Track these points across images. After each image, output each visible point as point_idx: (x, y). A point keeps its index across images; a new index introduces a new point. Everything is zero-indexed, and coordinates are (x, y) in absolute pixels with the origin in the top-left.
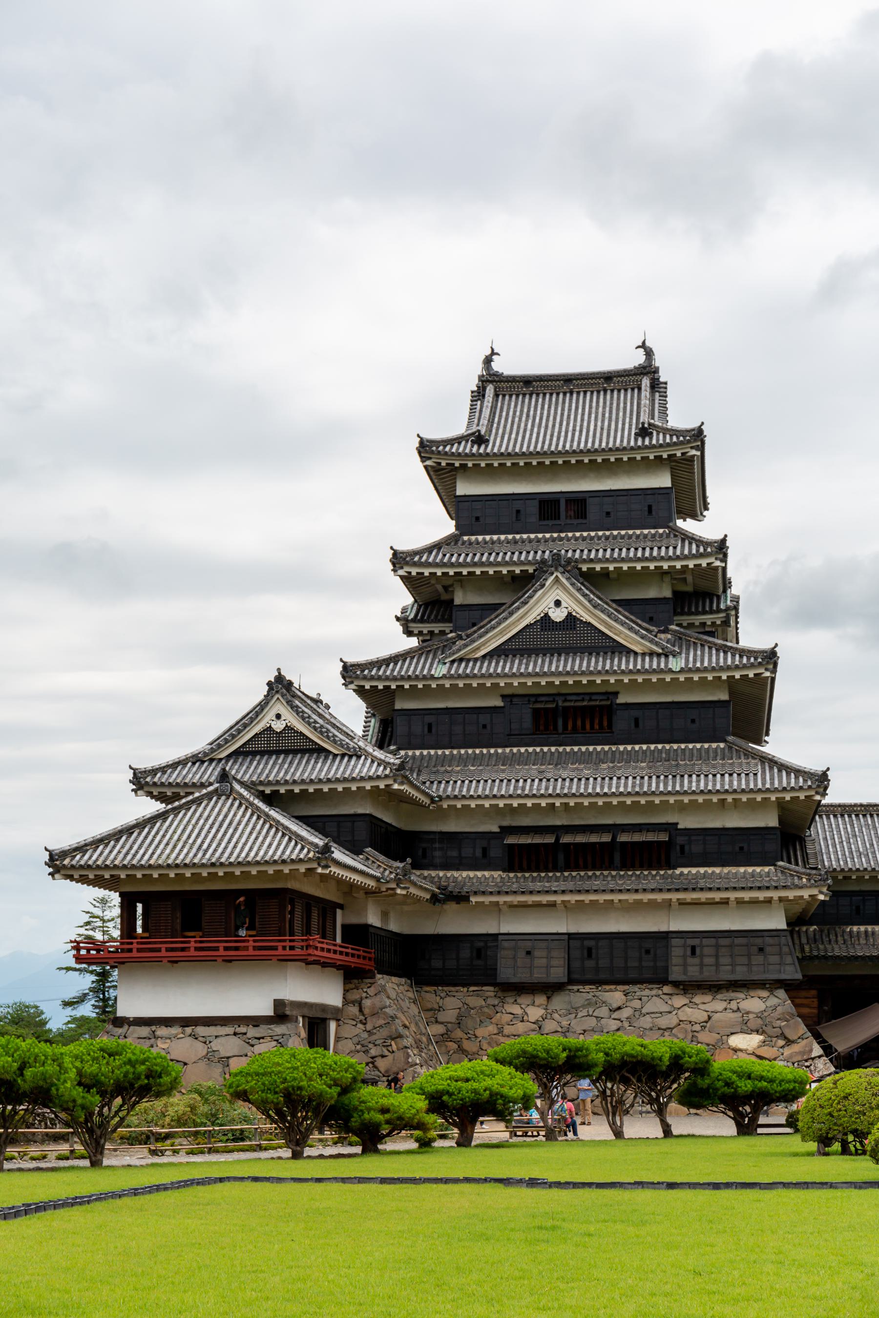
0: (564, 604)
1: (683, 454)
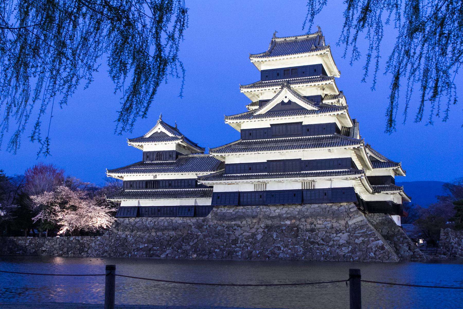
0: (287, 97)
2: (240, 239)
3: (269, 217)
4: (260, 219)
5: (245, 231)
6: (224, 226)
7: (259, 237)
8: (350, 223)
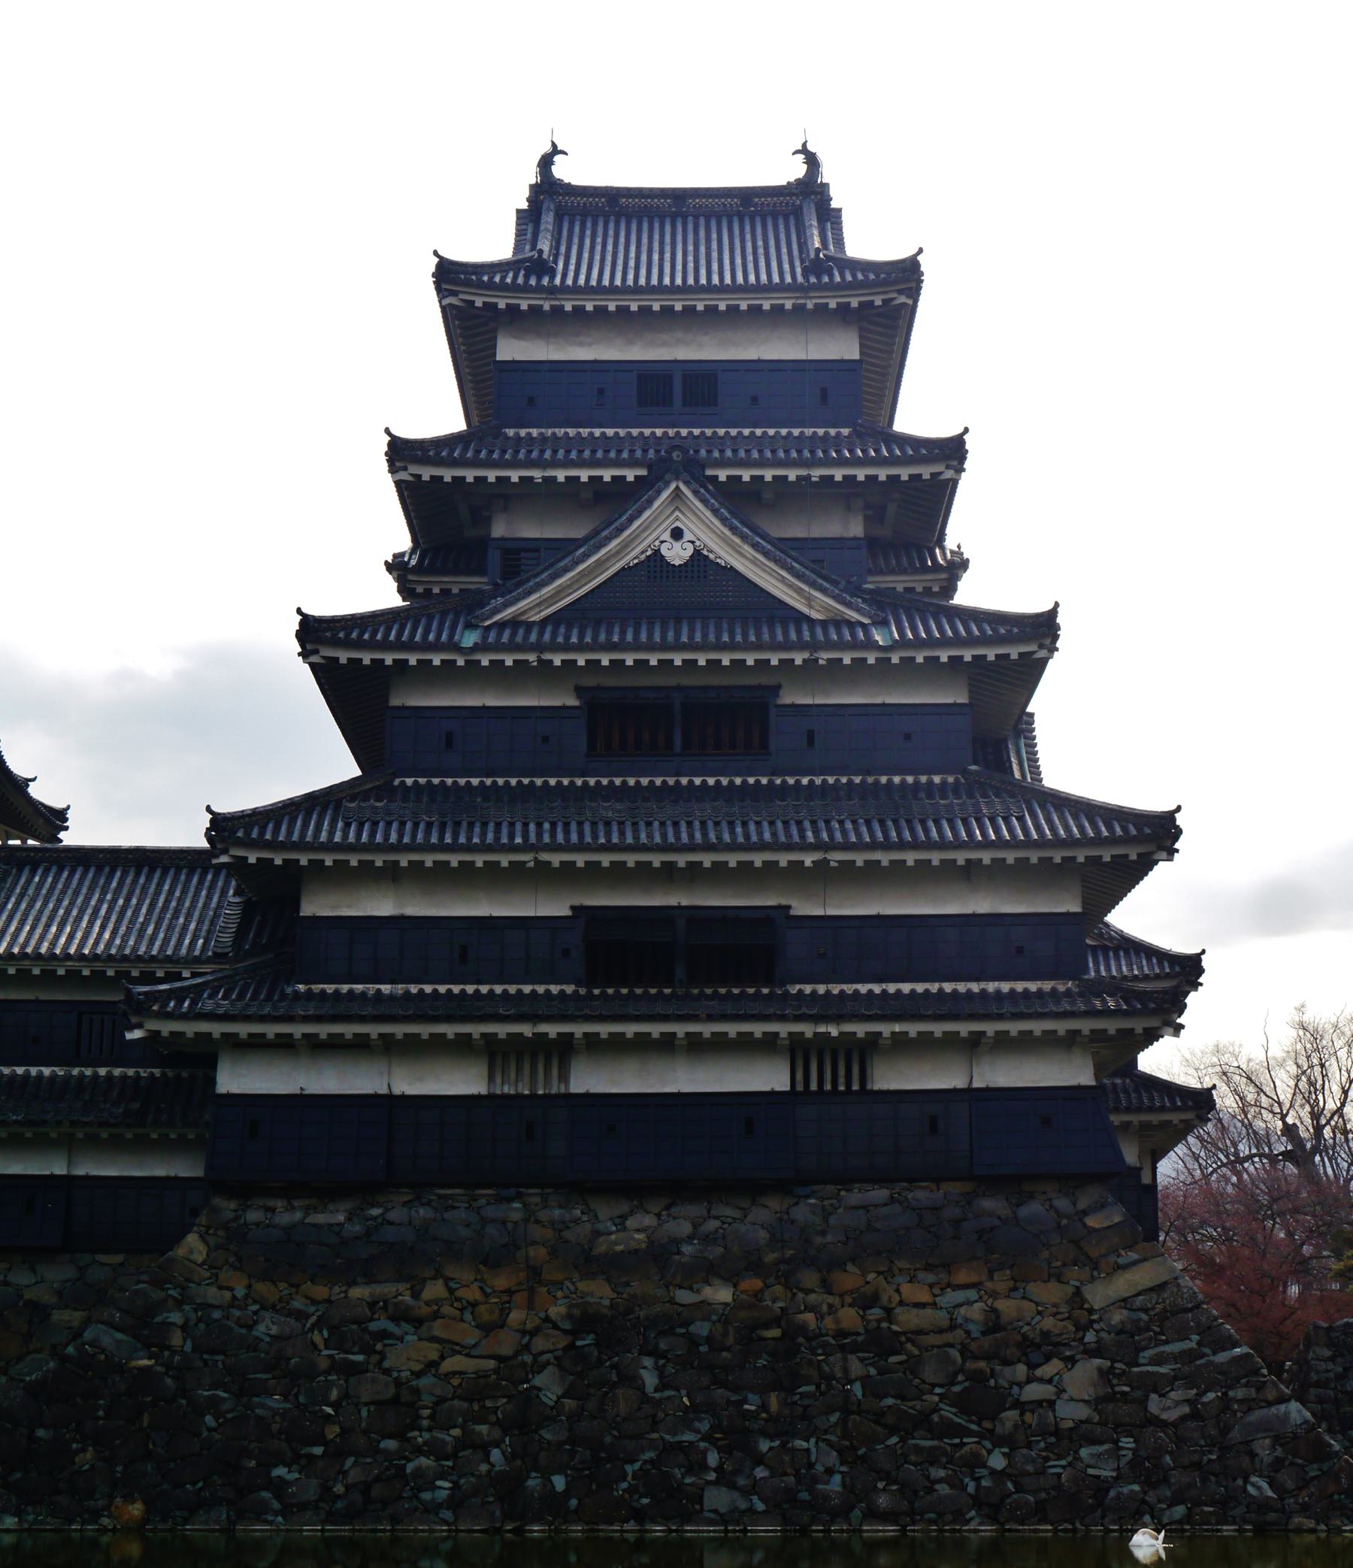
0: (688, 536)
2: (427, 1399)
3: (591, 1262)
4: (535, 1272)
5: (450, 1347)
6: (301, 1316)
7: (549, 1385)
8: (1100, 1294)
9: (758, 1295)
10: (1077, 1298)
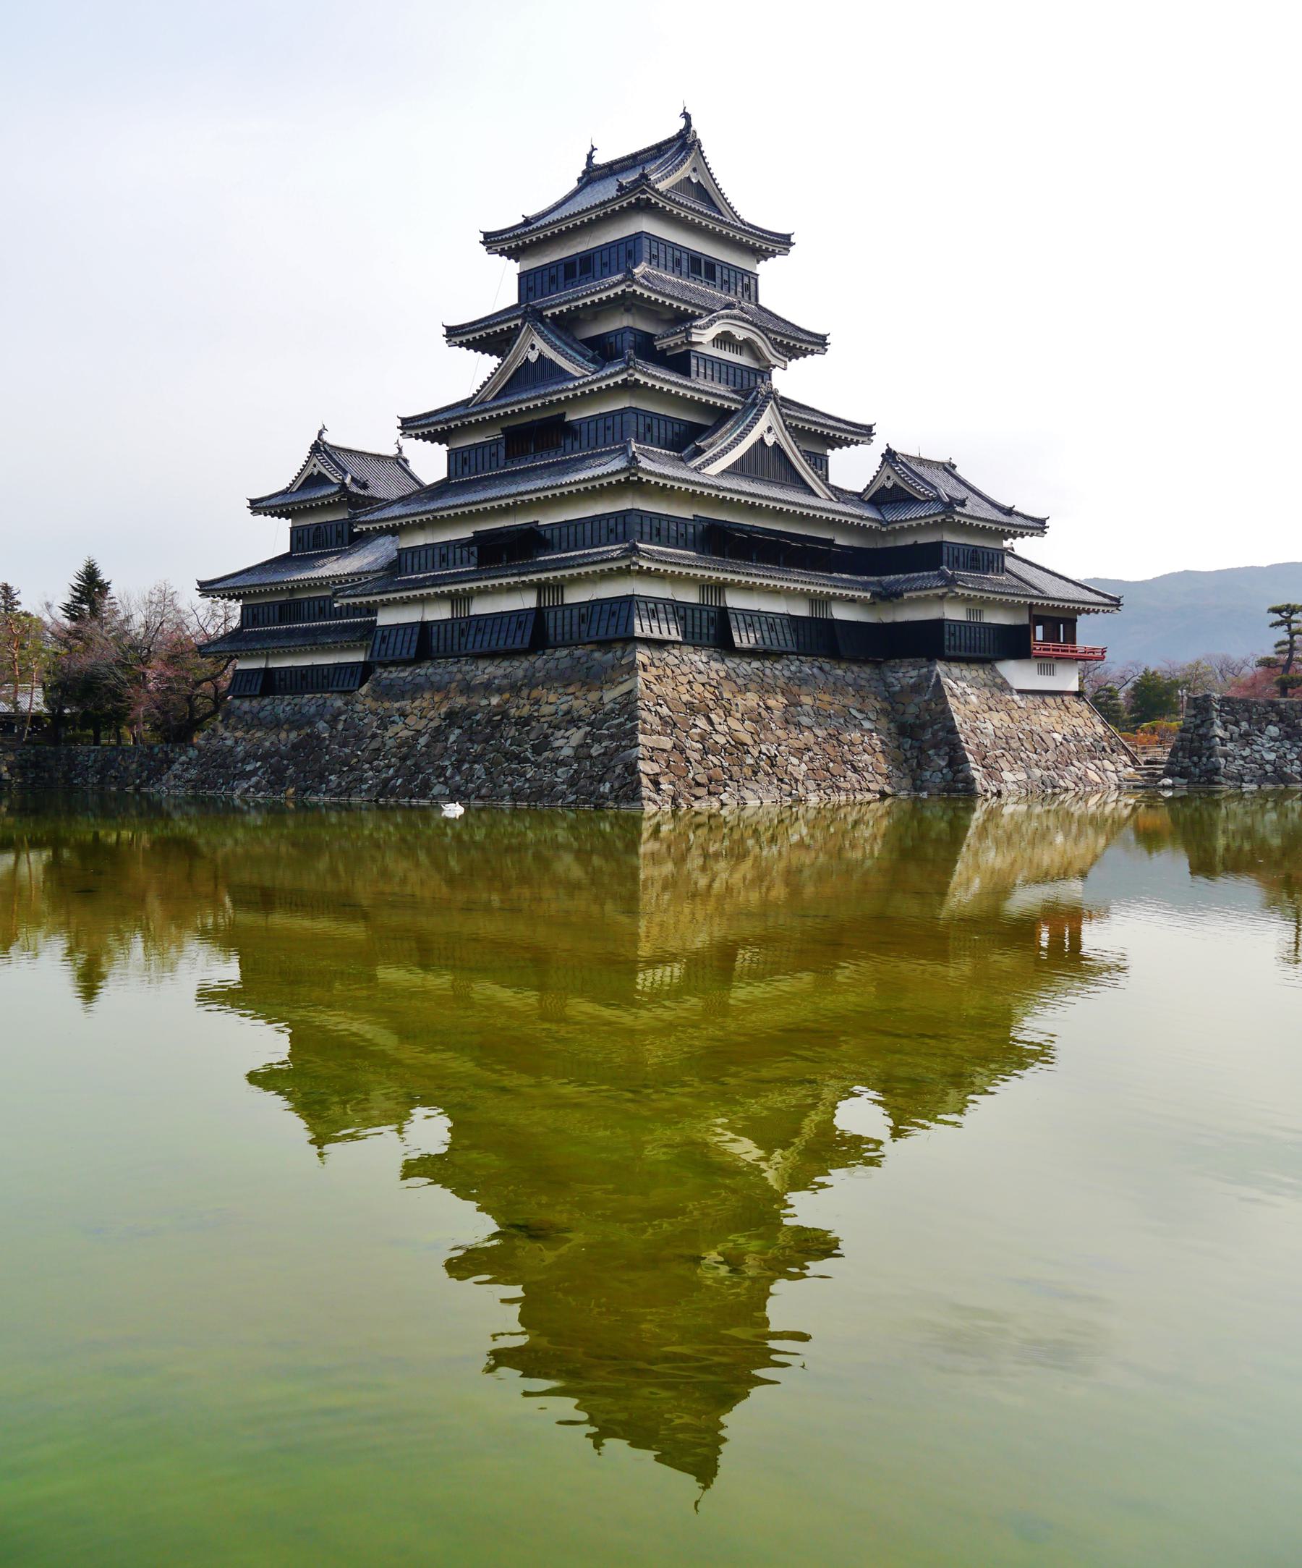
1: (638, 199)
3: (467, 689)
7: (423, 740)
9: (507, 701)
10: (601, 698)
